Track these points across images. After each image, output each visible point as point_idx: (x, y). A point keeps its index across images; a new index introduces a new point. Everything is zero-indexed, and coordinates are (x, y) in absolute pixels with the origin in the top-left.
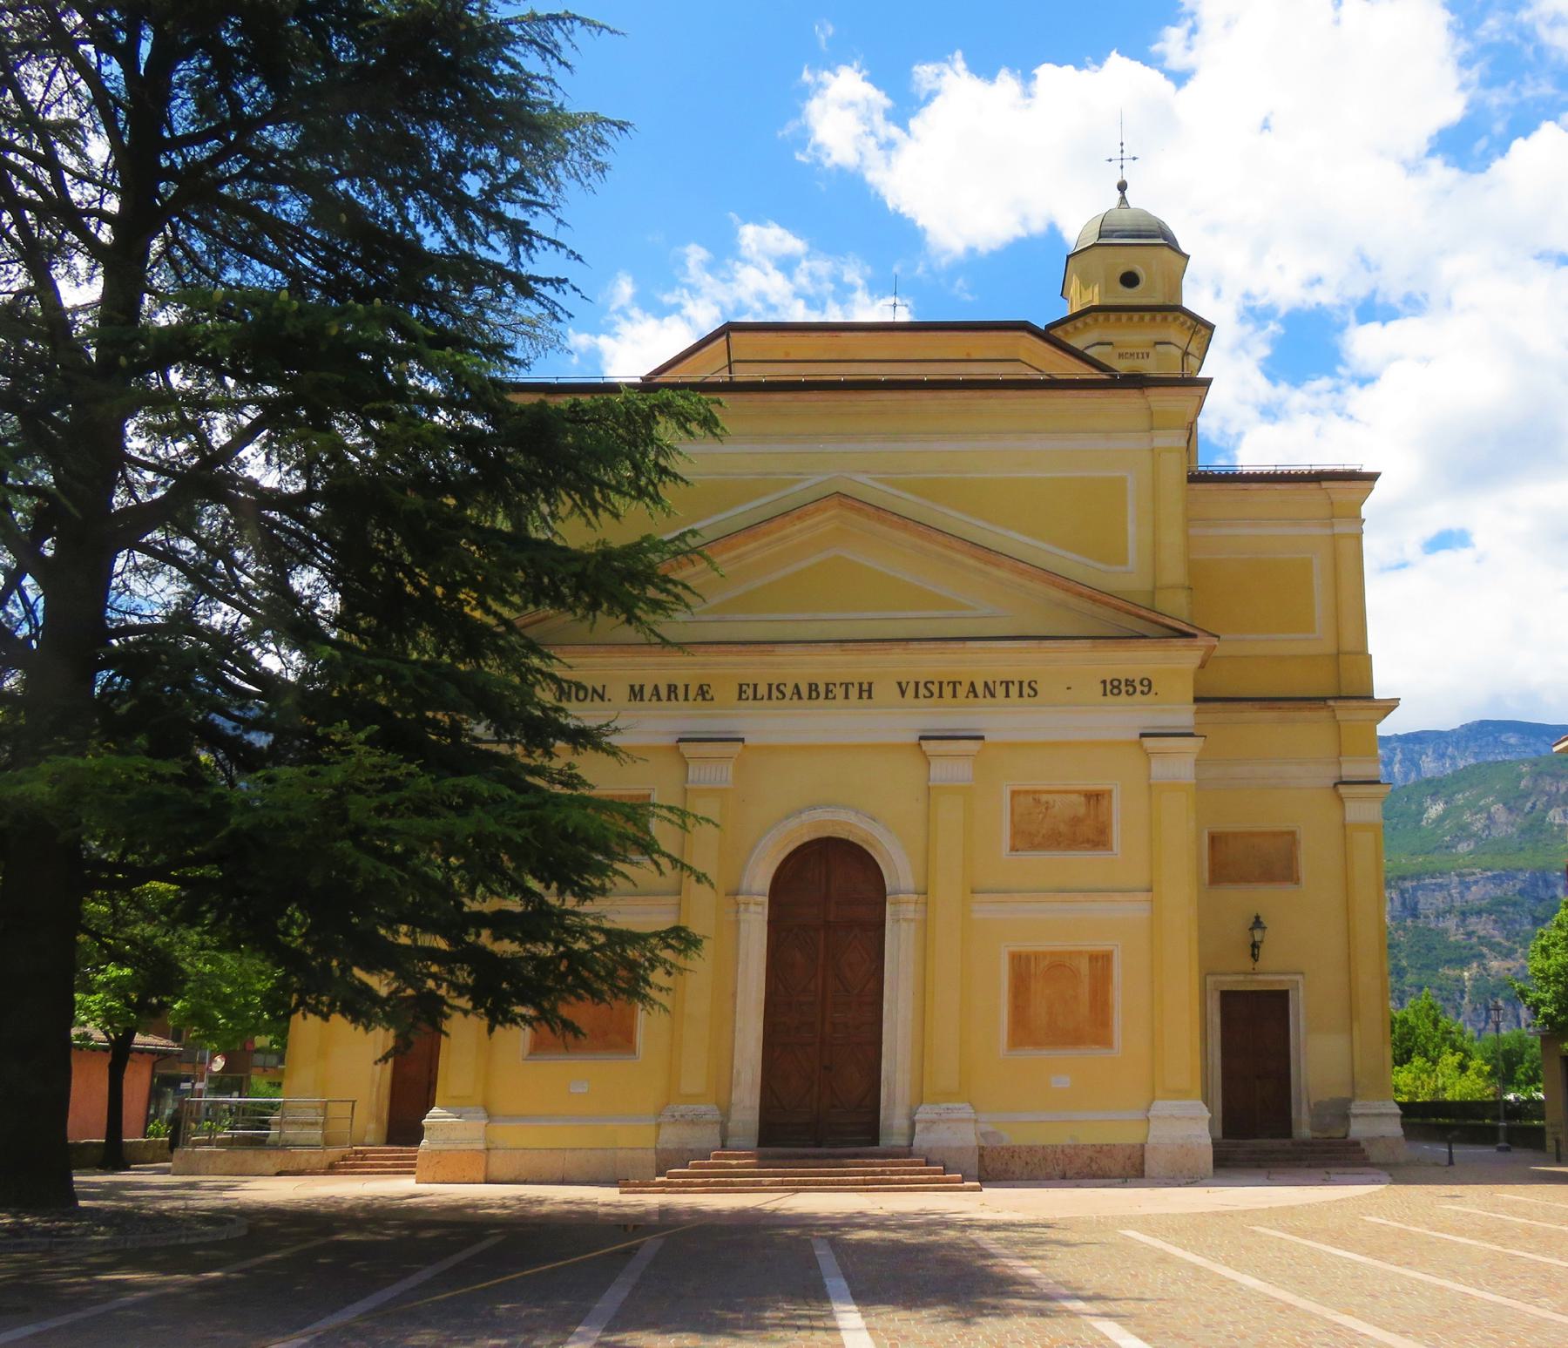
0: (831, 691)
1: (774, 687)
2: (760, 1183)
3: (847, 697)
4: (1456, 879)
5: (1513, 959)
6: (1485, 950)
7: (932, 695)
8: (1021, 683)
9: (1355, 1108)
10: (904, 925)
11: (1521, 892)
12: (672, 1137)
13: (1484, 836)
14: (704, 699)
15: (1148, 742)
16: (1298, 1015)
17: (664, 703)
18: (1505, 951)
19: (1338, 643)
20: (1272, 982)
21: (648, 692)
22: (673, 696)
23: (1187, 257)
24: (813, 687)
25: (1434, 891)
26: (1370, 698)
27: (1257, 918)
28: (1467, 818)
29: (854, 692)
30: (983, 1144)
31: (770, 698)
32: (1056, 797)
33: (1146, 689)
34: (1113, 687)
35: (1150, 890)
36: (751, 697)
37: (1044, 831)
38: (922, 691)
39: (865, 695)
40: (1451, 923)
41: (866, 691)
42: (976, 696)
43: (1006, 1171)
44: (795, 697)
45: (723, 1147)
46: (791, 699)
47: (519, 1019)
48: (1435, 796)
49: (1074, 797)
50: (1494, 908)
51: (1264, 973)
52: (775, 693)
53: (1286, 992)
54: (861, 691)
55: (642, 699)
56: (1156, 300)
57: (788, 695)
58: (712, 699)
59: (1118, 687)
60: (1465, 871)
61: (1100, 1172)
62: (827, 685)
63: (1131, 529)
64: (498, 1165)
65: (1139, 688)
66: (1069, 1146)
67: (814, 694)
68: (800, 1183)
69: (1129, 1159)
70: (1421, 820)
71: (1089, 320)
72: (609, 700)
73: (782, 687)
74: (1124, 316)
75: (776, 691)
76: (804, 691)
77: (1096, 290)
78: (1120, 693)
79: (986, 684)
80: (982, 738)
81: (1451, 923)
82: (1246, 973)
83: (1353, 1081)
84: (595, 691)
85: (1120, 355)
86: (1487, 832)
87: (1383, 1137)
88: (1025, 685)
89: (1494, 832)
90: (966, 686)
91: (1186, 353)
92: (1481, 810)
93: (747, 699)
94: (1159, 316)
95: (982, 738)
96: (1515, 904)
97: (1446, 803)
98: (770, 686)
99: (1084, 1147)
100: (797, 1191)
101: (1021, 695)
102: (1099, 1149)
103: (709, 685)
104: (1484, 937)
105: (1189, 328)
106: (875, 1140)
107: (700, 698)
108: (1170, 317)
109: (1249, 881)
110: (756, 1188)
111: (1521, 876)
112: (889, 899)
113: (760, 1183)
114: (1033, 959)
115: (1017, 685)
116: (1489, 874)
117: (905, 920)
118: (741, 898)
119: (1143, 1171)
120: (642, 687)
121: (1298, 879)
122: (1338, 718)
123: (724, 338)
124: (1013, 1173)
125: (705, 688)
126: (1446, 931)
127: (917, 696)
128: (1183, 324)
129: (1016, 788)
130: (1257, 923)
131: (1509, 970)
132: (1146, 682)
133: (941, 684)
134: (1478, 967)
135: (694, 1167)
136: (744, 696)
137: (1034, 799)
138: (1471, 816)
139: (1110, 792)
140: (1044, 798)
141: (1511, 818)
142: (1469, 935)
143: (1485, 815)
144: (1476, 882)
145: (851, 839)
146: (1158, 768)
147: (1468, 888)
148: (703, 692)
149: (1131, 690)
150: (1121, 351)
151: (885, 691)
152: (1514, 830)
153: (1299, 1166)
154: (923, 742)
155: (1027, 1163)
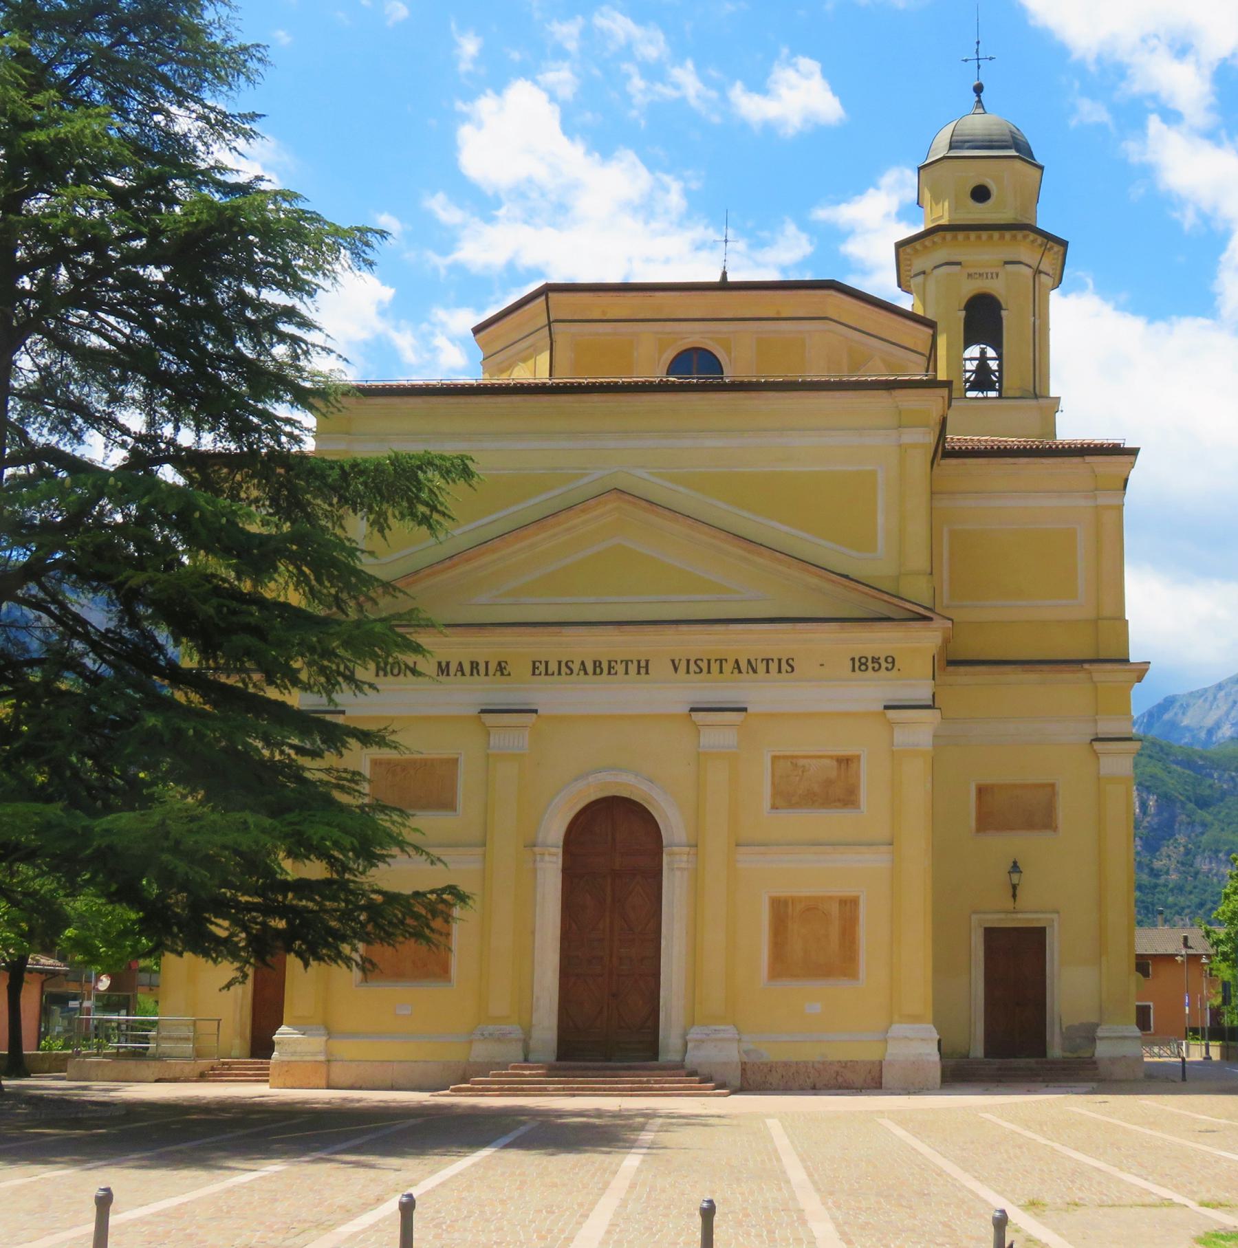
0: (613, 668)
1: (563, 665)
2: (545, 1089)
3: (627, 673)
7: (701, 670)
8: (780, 661)
9: (1100, 1033)
12: (481, 1051)
15: (891, 714)
17: (468, 677)
22: (475, 671)
23: (1041, 168)
24: (598, 663)
26: (1127, 661)
27: (1015, 863)
29: (633, 668)
30: (745, 1059)
31: (559, 673)
33: (890, 666)
34: (861, 664)
35: (891, 844)
36: (543, 672)
38: (693, 667)
39: (643, 671)
41: (644, 667)
42: (740, 672)
44: (582, 673)
45: (526, 1060)
46: (578, 674)
47: (326, 958)
49: (827, 762)
51: (1026, 912)
52: (564, 669)
53: (1044, 929)
54: (639, 667)
56: (1006, 215)
57: (575, 671)
58: (509, 674)
59: (865, 664)
62: (610, 662)
63: (880, 519)
64: (338, 1072)
65: (884, 665)
66: (819, 1062)
67: (598, 670)
68: (577, 1089)
69: (870, 1073)
71: (937, 238)
73: (570, 664)
74: (973, 235)
75: (566, 667)
76: (590, 669)
77: (946, 204)
78: (867, 669)
79: (749, 662)
80: (745, 710)
82: (1007, 912)
83: (1101, 1007)
84: (407, 666)
85: (970, 275)
87: (1125, 1056)
90: (731, 663)
91: (1038, 272)
93: (540, 674)
94: (1008, 235)
95: (745, 710)
98: (560, 663)
99: (831, 1063)
100: (574, 1096)
101: (780, 671)
102: (845, 1065)
103: (506, 662)
105: (1041, 245)
106: (655, 1055)
107: (499, 673)
108: (1020, 234)
109: (1011, 829)
110: (542, 1092)
112: (665, 850)
113: (545, 1089)
115: (776, 661)
117: (679, 869)
118: (537, 849)
119: (881, 1083)
120: (448, 664)
121: (1057, 827)
122: (1095, 679)
123: (543, 298)
124: (771, 1084)
125: (503, 664)
127: (688, 672)
128: (1034, 241)
129: (778, 754)
130: (1015, 868)
132: (890, 660)
133: (709, 661)
135: (494, 1076)
136: (537, 672)
137: (791, 763)
139: (858, 757)
140: (801, 762)
145: (632, 798)
146: (900, 737)
148: (501, 668)
149: (876, 666)
150: (972, 271)
151: (661, 668)
153: (1034, 1081)
154: (693, 713)
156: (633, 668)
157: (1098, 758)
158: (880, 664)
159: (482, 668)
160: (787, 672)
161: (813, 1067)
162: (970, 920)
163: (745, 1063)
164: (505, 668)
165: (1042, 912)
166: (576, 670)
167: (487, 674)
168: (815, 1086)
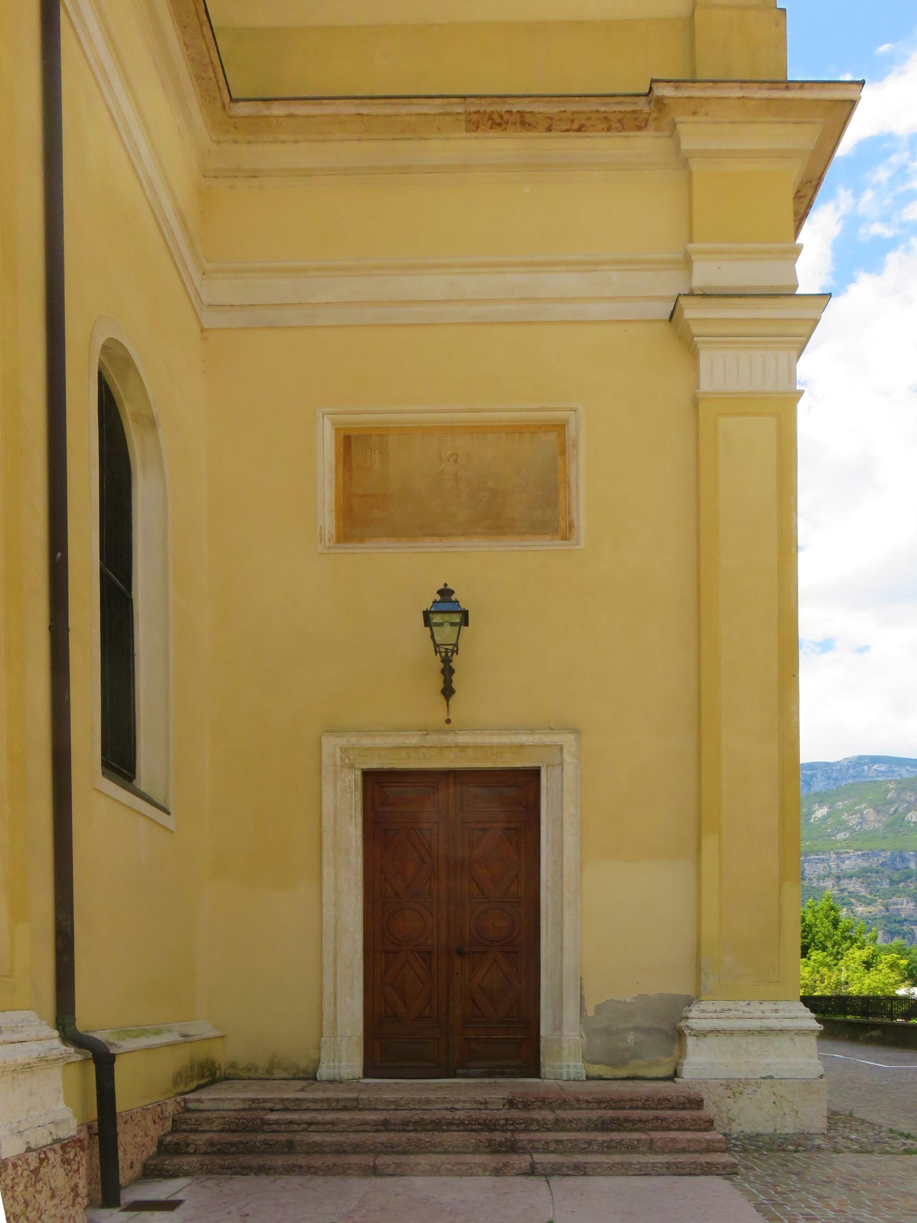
4: (834, 856)
5: (873, 906)
6: (853, 900)
11: (883, 864)
13: (857, 829)
18: (867, 901)
25: (817, 863)
28: (845, 817)
40: (829, 883)
48: (821, 803)
50: (863, 875)
60: (840, 851)
70: (810, 819)
81: (829, 883)
86: (859, 827)
89: (864, 826)
92: (856, 812)
96: (877, 872)
97: (830, 808)
104: (853, 893)
111: (883, 854)
116: (859, 853)
126: (825, 888)
131: (870, 912)
134: (847, 911)
138: (848, 816)
141: (879, 818)
142: (842, 890)
143: (859, 816)
144: (849, 858)
147: (843, 862)
152: (880, 825)
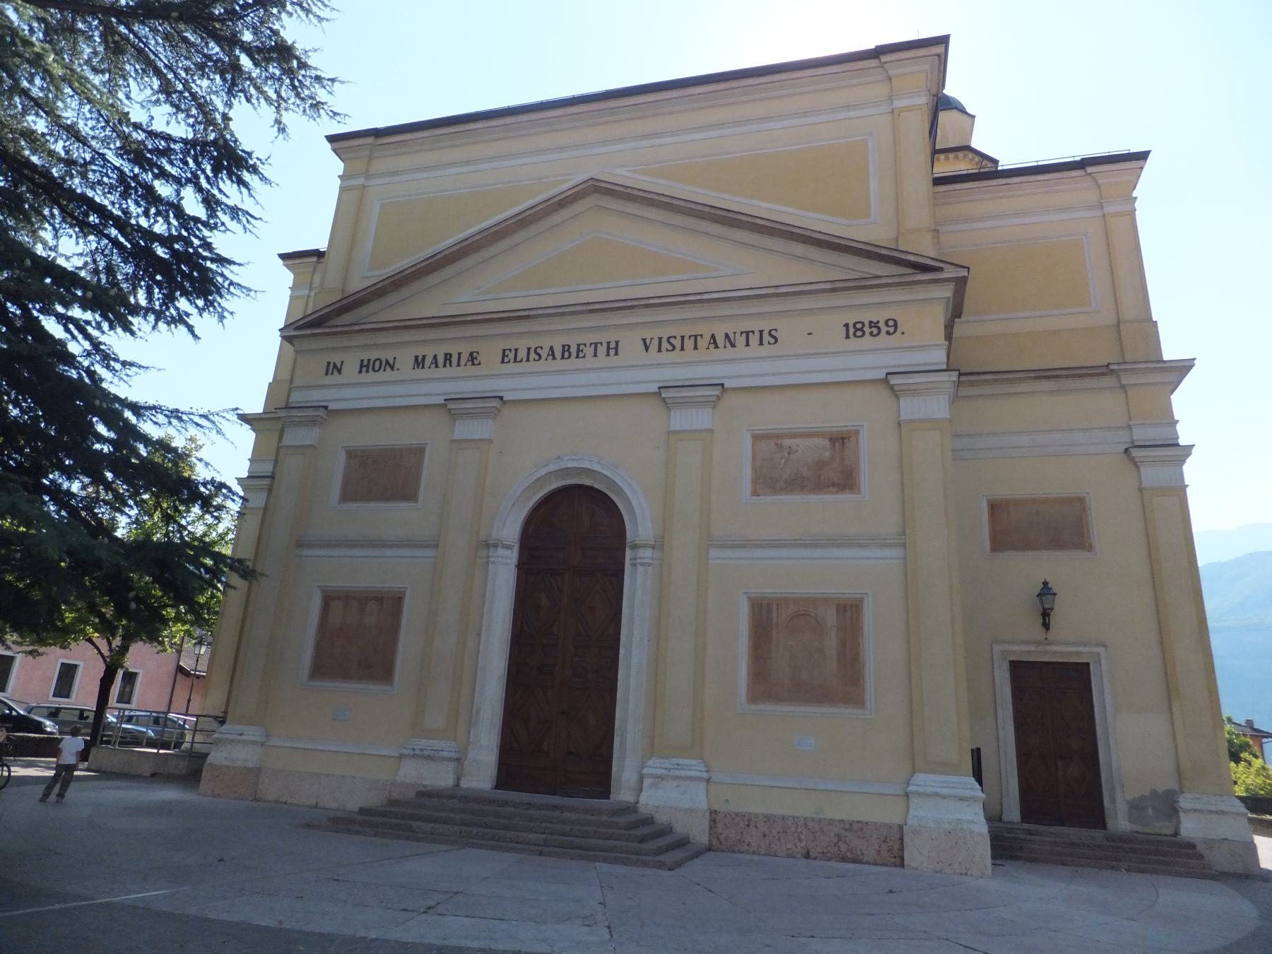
0: (582, 351)
1: (532, 351)
3: (595, 355)
7: (674, 348)
8: (761, 332)
10: (640, 569)
14: (473, 364)
16: (1102, 692)
19: (1118, 314)
20: (1070, 654)
21: (428, 360)
22: (448, 362)
27: (1045, 584)
29: (602, 350)
31: (528, 360)
32: (797, 441)
33: (892, 330)
34: (855, 330)
36: (512, 360)
37: (785, 476)
38: (665, 345)
39: (612, 352)
41: (613, 349)
42: (716, 347)
43: (741, 841)
49: (819, 441)
52: (533, 355)
55: (423, 367)
58: (479, 364)
61: (849, 855)
62: (579, 345)
63: (873, 184)
65: (884, 329)
67: (566, 354)
72: (398, 370)
73: (539, 350)
75: (535, 354)
78: (863, 335)
79: (727, 336)
82: (1037, 643)
88: (765, 335)
90: (707, 338)
93: (509, 362)
101: (761, 344)
102: (850, 826)
103: (478, 352)
107: (470, 363)
109: (1035, 549)
114: (775, 607)
115: (757, 335)
117: (642, 564)
119: (902, 858)
120: (424, 357)
122: (1123, 382)
125: (475, 354)
127: (660, 351)
132: (891, 323)
133: (683, 337)
136: (506, 360)
137: (776, 444)
140: (786, 442)
148: (472, 358)
149: (875, 331)
155: (764, 835)
156: (602, 350)
157: (1138, 467)
158: (879, 329)
159: (454, 360)
160: (769, 343)
161: (806, 825)
162: (992, 649)
163: (715, 811)
164: (476, 358)
165: (1085, 645)
166: (544, 355)
167: (458, 365)
168: (808, 853)
